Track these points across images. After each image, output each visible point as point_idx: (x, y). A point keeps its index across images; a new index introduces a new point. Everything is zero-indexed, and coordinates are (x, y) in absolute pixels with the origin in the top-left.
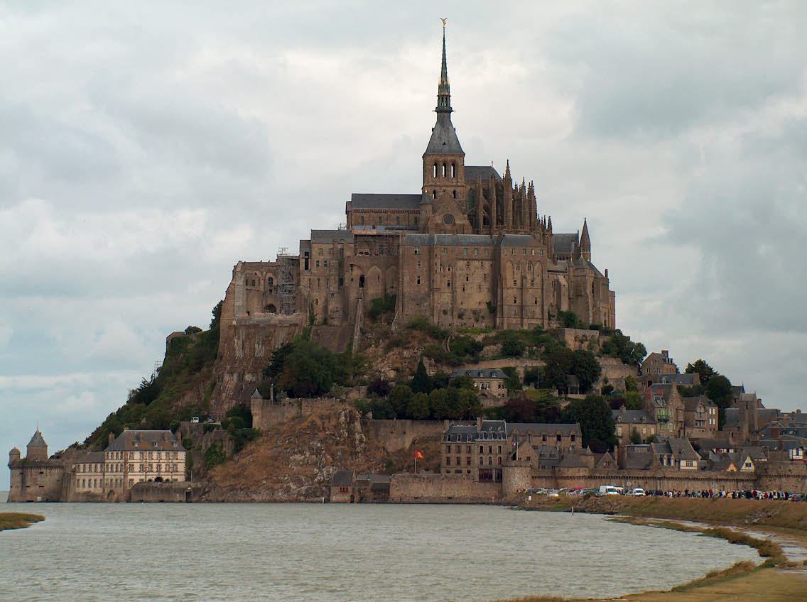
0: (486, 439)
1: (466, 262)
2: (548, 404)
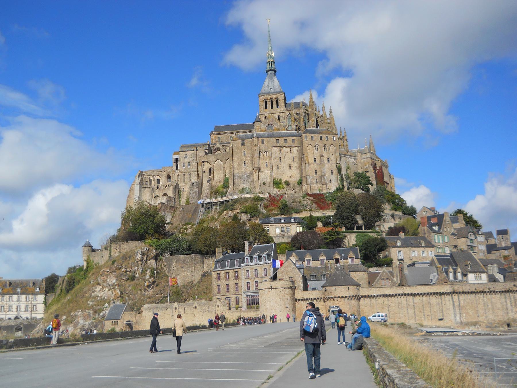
0: (251, 262)
1: (279, 149)
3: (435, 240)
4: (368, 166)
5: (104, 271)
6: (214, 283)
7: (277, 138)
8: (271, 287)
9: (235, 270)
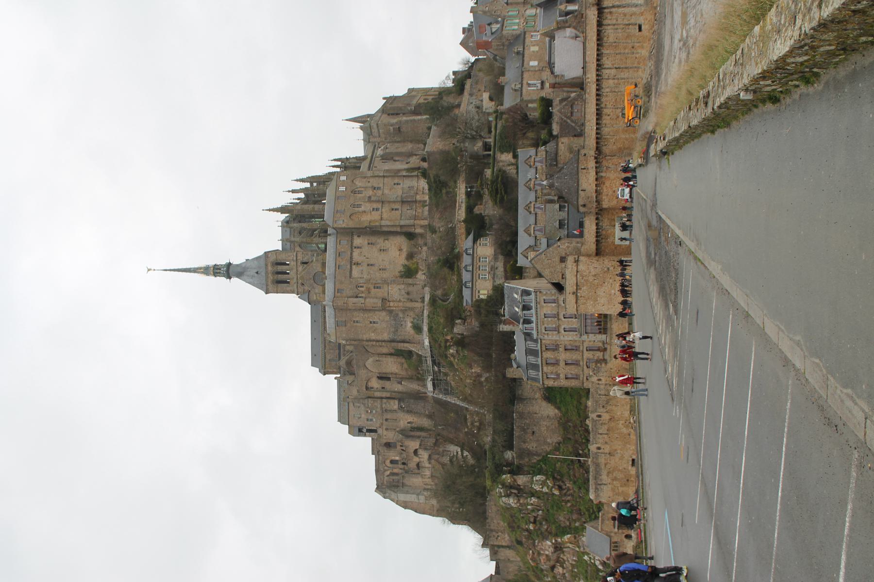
0: (533, 323)
1: (354, 267)
2: (497, 190)
3: (513, 30)
4: (391, 126)
5: (531, 559)
6: (562, 384)
7: (337, 269)
8: (573, 293)
9: (544, 349)
